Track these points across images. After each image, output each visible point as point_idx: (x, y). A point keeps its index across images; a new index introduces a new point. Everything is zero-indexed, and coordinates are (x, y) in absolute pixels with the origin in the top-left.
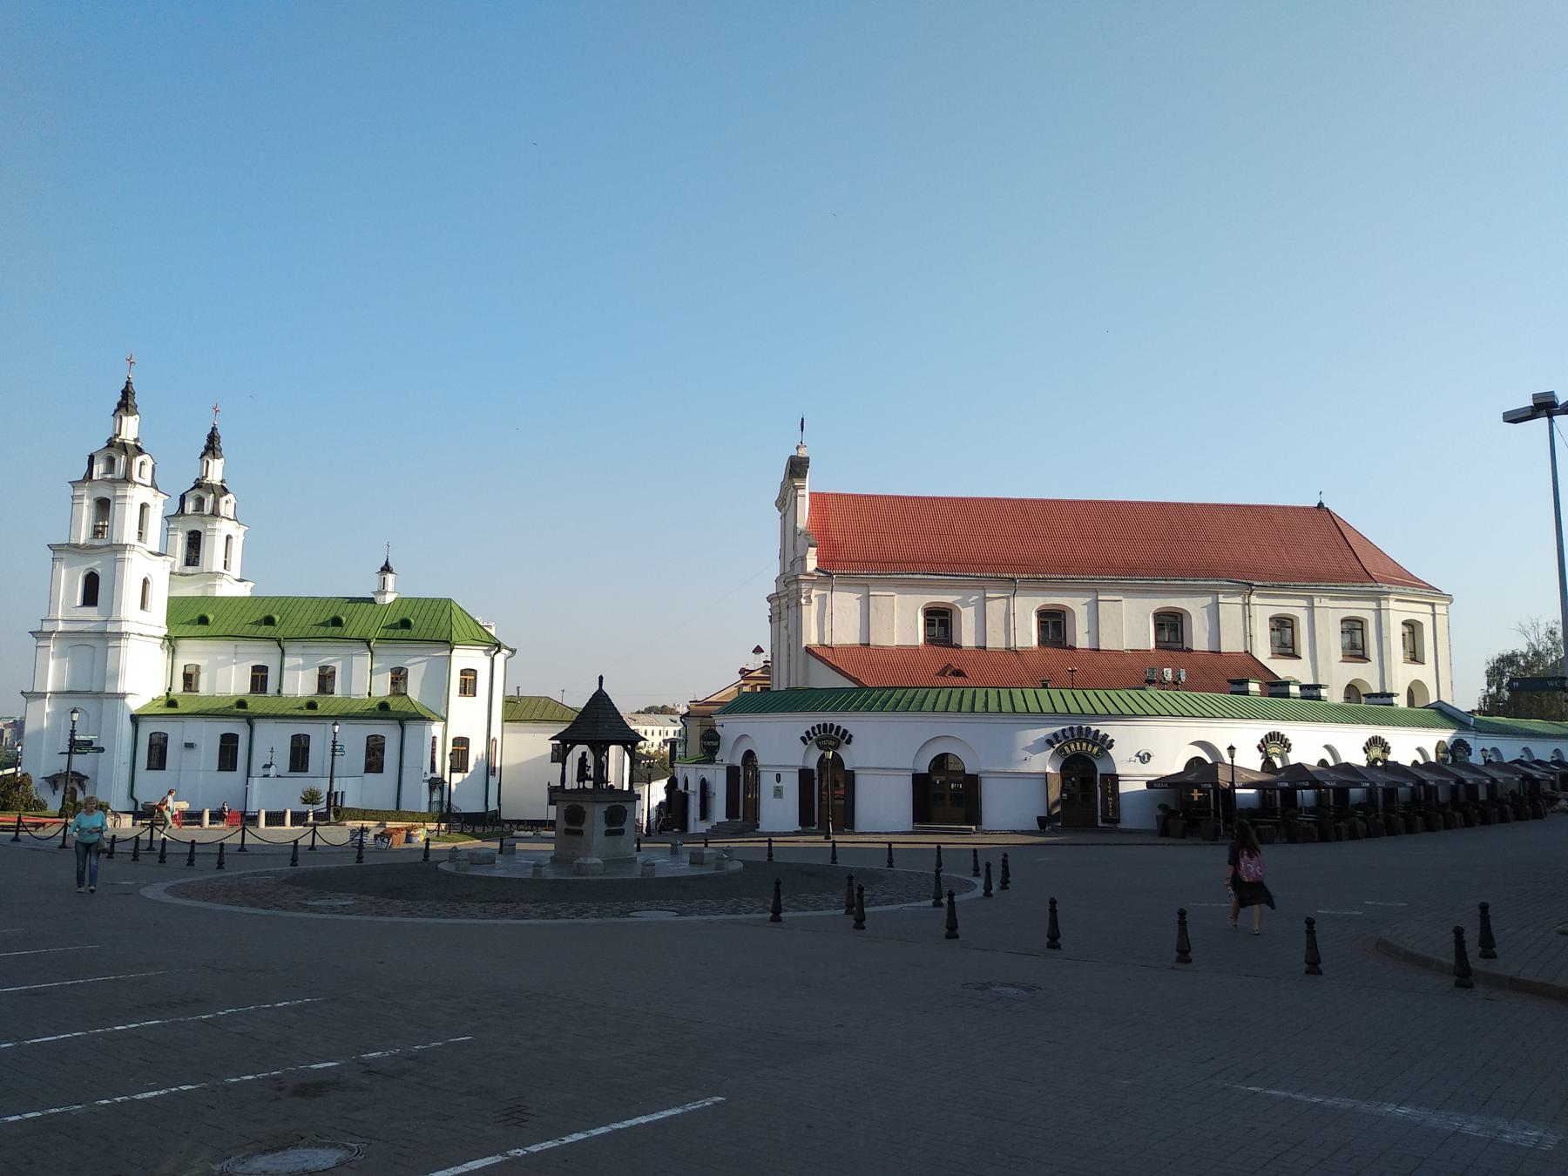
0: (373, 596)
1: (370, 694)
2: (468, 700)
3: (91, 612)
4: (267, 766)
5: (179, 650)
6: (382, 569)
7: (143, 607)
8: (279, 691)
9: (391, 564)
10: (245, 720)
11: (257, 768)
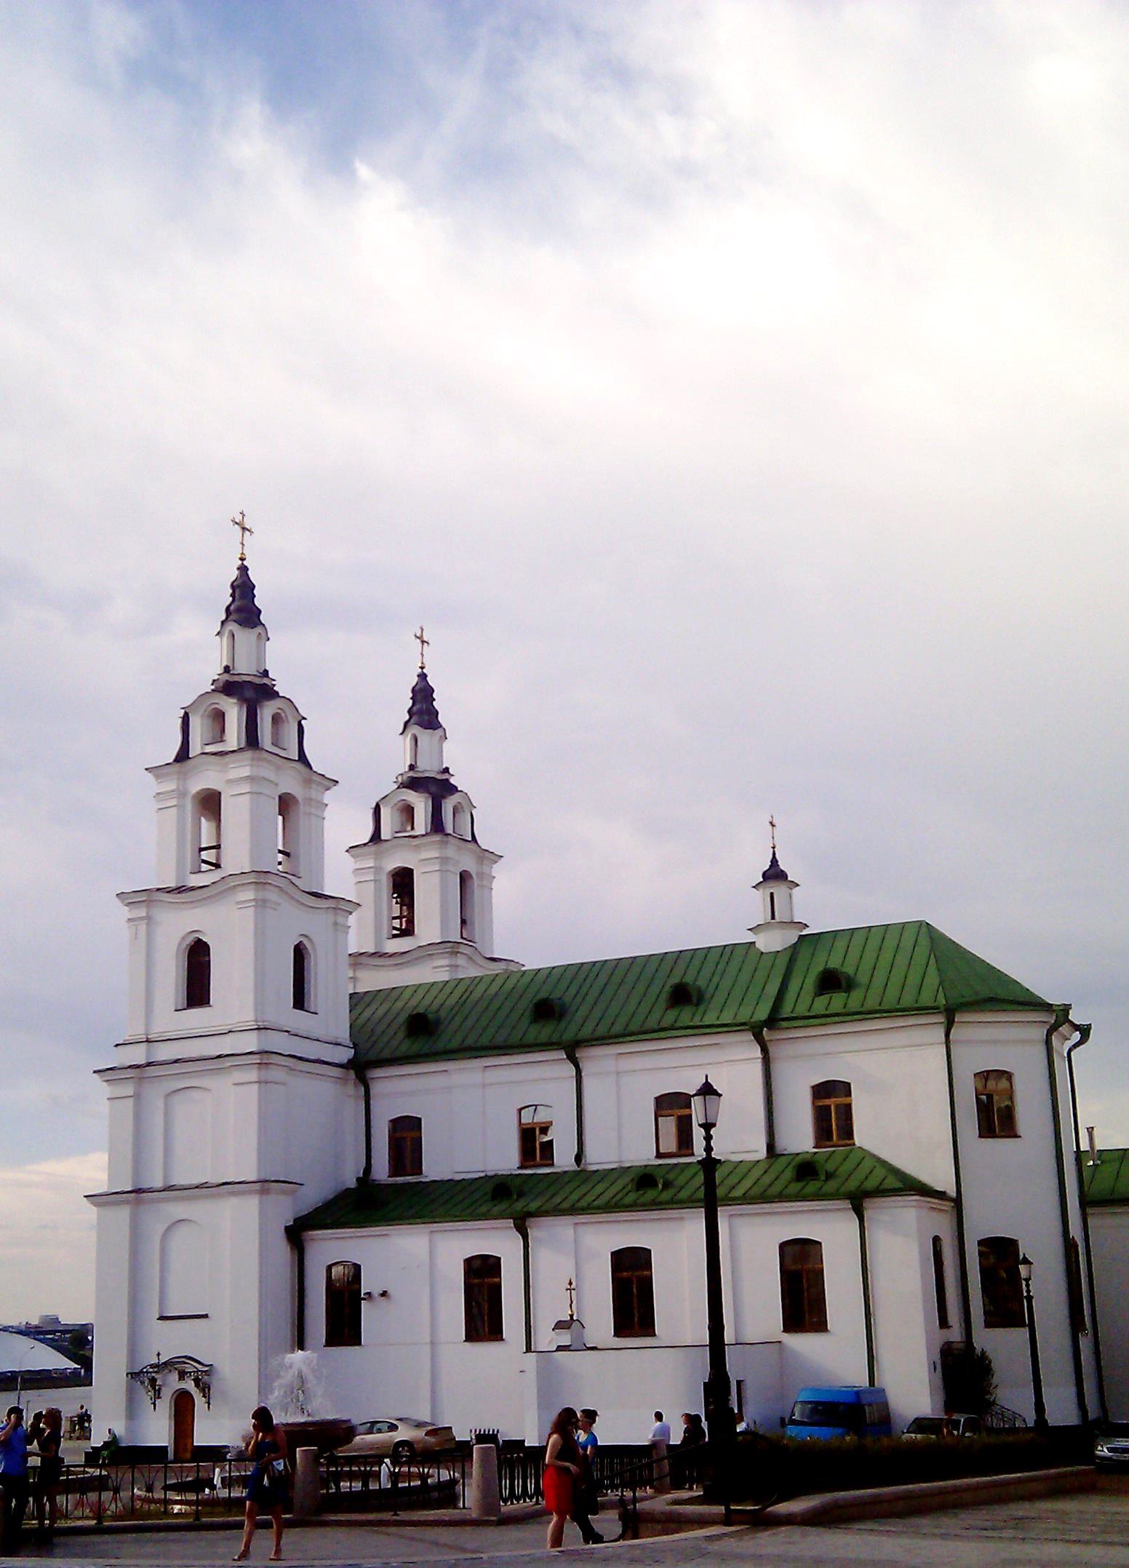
0: (750, 937)
1: (771, 1147)
2: (999, 1147)
3: (197, 1018)
4: (560, 1325)
5: (376, 1088)
6: (766, 876)
7: (300, 1001)
8: (579, 1158)
9: (783, 866)
10: (510, 1223)
11: (546, 1338)
